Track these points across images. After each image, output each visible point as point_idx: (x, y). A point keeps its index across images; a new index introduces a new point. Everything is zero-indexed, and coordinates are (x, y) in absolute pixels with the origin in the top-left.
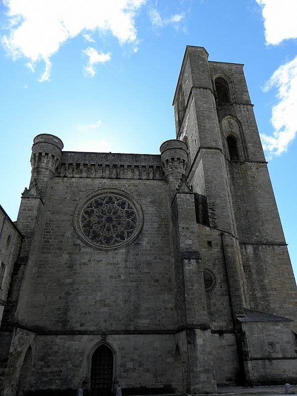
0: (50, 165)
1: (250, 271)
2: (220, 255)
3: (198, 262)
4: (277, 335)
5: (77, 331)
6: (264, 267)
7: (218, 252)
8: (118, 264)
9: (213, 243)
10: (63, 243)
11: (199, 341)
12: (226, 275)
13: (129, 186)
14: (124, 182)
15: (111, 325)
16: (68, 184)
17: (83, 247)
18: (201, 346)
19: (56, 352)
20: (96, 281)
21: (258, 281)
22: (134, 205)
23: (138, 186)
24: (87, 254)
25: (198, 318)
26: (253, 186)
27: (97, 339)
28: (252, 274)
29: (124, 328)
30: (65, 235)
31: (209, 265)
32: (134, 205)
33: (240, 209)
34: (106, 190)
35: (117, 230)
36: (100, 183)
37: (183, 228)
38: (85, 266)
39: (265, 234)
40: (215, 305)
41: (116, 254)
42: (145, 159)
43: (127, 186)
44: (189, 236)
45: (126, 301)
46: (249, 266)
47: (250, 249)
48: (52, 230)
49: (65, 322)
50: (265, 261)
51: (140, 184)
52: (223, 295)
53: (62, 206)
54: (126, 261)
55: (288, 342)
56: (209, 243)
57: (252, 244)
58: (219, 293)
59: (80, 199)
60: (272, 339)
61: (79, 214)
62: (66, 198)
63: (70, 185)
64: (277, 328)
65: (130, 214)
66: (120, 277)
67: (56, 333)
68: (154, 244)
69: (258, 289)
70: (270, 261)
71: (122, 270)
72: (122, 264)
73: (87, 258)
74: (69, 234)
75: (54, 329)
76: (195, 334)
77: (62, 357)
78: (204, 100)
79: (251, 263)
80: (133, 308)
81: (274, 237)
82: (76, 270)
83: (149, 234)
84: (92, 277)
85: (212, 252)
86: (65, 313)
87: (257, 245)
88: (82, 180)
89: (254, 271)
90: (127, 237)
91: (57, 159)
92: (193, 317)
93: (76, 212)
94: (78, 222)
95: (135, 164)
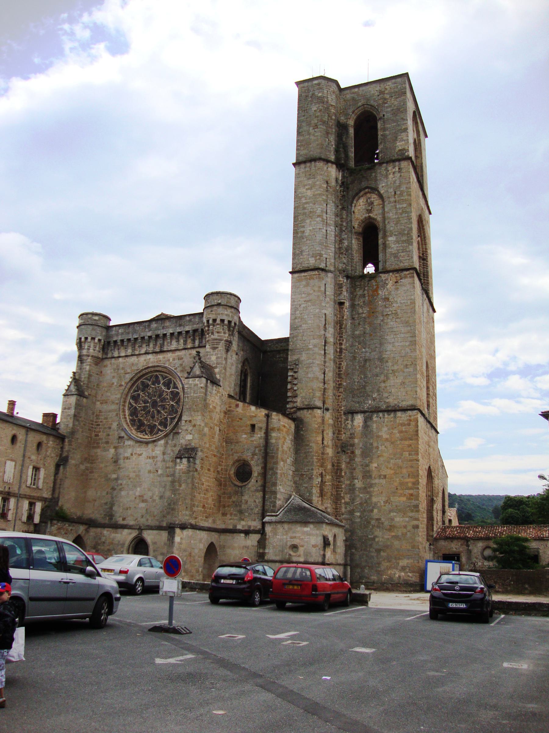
0: (91, 350)
1: (353, 452)
2: (262, 442)
3: (189, 461)
4: (303, 537)
5: (120, 525)
6: (375, 444)
7: (260, 438)
8: (157, 457)
9: (256, 426)
11: (177, 539)
12: (265, 468)
13: (174, 360)
14: (169, 355)
15: (147, 520)
16: (115, 367)
18: (178, 543)
19: (104, 543)
20: (136, 476)
24: (130, 448)
25: (180, 518)
26: (383, 316)
27: (134, 533)
29: (157, 523)
31: (247, 456)
33: (355, 358)
34: (149, 370)
36: (145, 360)
37: (186, 421)
38: (128, 461)
39: (386, 395)
40: (247, 502)
41: (156, 446)
42: (190, 321)
44: (191, 430)
45: (161, 497)
46: (353, 445)
47: (359, 419)
48: (101, 422)
49: (111, 516)
50: (378, 437)
51: (185, 355)
52: (257, 491)
54: (164, 454)
55: (314, 546)
56: (253, 426)
57: (364, 412)
58: (253, 489)
60: (296, 542)
62: (113, 384)
64: (306, 529)
65: (175, 396)
66: (157, 471)
67: (104, 526)
69: (360, 477)
70: (385, 436)
71: (160, 464)
72: (160, 458)
73: (129, 451)
74: (115, 425)
75: (103, 521)
76: (174, 533)
77: (108, 547)
79: (356, 441)
80: (166, 504)
81: (400, 397)
82: (120, 465)
84: (134, 472)
85: (253, 439)
86: (111, 508)
87: (369, 413)
88: (128, 359)
89: (358, 452)
91: (99, 340)
92: (175, 517)
95: (178, 330)
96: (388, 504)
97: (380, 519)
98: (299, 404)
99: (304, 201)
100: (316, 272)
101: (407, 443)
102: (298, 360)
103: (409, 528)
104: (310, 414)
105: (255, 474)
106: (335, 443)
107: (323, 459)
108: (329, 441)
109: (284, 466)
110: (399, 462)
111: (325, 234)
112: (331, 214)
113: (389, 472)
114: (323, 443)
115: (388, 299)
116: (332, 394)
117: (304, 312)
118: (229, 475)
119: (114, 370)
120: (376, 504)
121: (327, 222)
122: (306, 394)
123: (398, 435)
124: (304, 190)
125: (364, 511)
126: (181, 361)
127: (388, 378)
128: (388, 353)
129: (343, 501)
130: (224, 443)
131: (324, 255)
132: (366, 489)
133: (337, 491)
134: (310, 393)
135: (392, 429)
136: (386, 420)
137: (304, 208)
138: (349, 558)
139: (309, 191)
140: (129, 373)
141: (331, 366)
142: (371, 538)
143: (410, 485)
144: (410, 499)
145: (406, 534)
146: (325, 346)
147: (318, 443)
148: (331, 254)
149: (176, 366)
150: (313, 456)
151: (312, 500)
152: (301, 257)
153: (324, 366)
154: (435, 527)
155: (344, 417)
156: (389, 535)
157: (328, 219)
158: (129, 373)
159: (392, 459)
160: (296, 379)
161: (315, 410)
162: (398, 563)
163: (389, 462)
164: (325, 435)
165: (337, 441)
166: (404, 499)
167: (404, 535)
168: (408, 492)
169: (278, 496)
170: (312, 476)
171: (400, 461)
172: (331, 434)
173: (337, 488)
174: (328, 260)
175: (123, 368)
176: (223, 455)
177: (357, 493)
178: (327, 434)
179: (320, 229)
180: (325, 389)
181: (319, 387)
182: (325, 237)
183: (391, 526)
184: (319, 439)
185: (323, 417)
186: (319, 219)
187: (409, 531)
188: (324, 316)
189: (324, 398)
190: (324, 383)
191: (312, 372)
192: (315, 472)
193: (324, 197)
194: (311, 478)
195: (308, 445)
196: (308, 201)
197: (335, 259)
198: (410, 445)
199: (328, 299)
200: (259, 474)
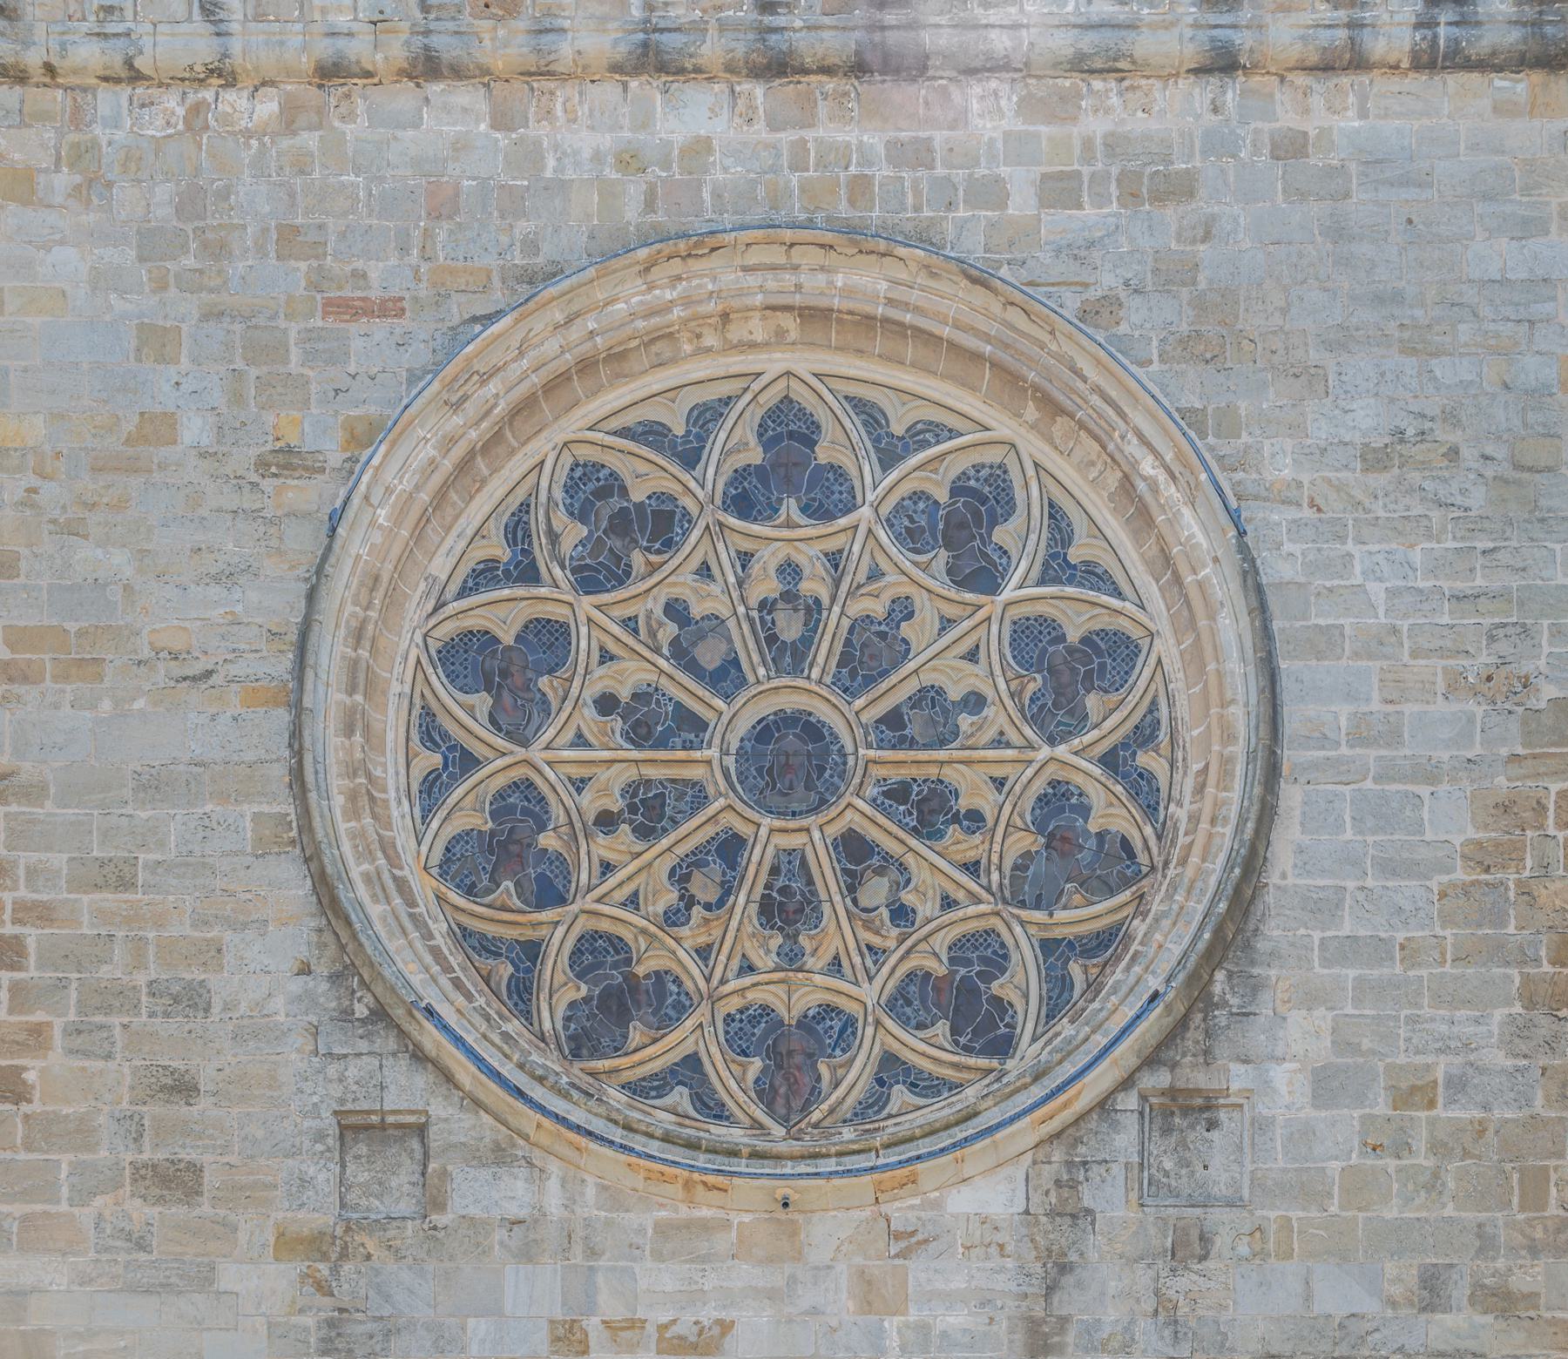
10: (203, 1103)
17: (474, 1157)
22: (1142, 517)
23: (1179, 188)
24: (527, 1254)
30: (221, 985)
32: (1142, 517)
35: (901, 914)
36: (630, 161)
41: (908, 1242)
43: (1021, 202)
48: (41, 914)
53: (119, 559)
59: (364, 436)
61: (360, 679)
62: (159, 427)
63: (190, 204)
68: (1416, 1094)
83: (1345, 950)
90: (1053, 1010)
93: (331, 651)
94: (366, 798)
119: (152, 244)
126: (1170, 214)
140: (390, 308)
149: (1108, 280)
158: (390, 308)
175: (289, 240)
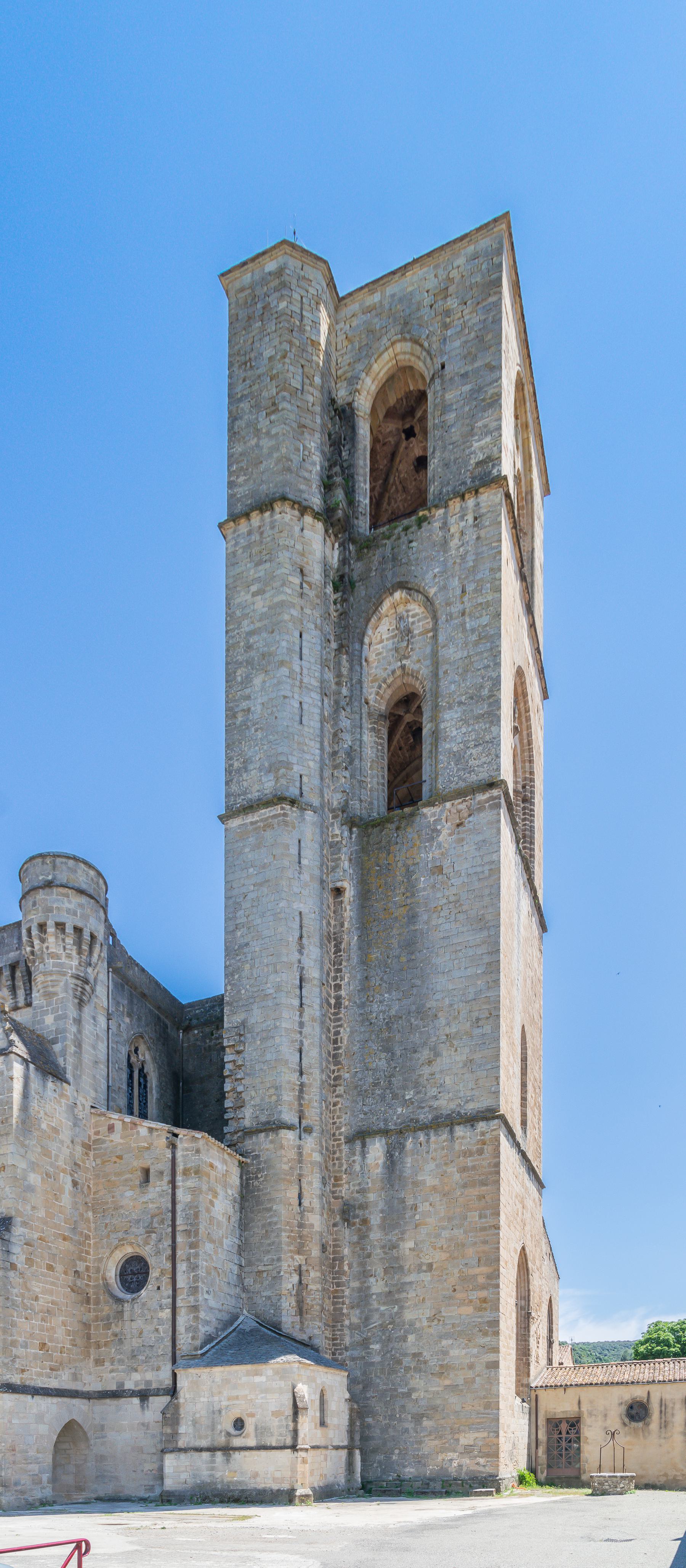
21: (383, 1247)
28: (369, 1229)
39: (433, 1091)
78: (261, 571)
96: (436, 1322)
97: (420, 1354)
98: (247, 1123)
99: (247, 629)
100: (277, 810)
101: (475, 1192)
102: (244, 1023)
103: (479, 1368)
104: (272, 1142)
105: (154, 1274)
106: (329, 1203)
107: (301, 1237)
108: (312, 1199)
109: (216, 1252)
110: (458, 1233)
111: (297, 711)
112: (313, 660)
113: (438, 1257)
114: (300, 1204)
115: (440, 869)
116: (317, 1098)
117: (254, 910)
118: (104, 1278)
120: (412, 1324)
121: (301, 682)
122: (262, 1099)
123: (457, 1177)
124: (249, 597)
125: (389, 1340)
127: (437, 1054)
128: (438, 996)
129: (347, 1322)
130: (90, 1214)
131: (296, 768)
132: (391, 1296)
133: (334, 1304)
134: (270, 1096)
135: (446, 1164)
136: (433, 1146)
137: (249, 647)
138: (357, 1437)
139: (259, 597)
141: (313, 1033)
142: (403, 1394)
143: (481, 1280)
144: (480, 1309)
145: (473, 1381)
146: (301, 988)
147: (290, 1204)
148: (311, 764)
150: (280, 1230)
151: (280, 1323)
152: (245, 775)
153: (301, 1033)
154: (532, 1368)
155: (345, 1148)
156: (439, 1386)
157: (305, 671)
159: (444, 1228)
160: (239, 1067)
161: (284, 1133)
162: (458, 1440)
163: (438, 1236)
164: (304, 1185)
165: (332, 1200)
166: (469, 1310)
167: (469, 1382)
168: (475, 1295)
169: (202, 1315)
170: (279, 1272)
171: (462, 1231)
172: (317, 1184)
173: (334, 1297)
174: (305, 779)
176: (87, 1237)
177: (375, 1305)
178: (310, 1183)
179: (285, 697)
180: (302, 1085)
181: (289, 1082)
182: (297, 718)
183: (441, 1366)
184: (293, 1193)
185: (299, 1147)
186: (284, 671)
187: (478, 1375)
188: (297, 919)
189: (301, 1105)
190: (301, 1074)
191: (273, 1050)
192: (284, 1265)
193: (295, 612)
194: (277, 1278)
195: (270, 1210)
196: (258, 625)
197: (322, 778)
198: (481, 1197)
199: (306, 877)
200: (162, 1273)
